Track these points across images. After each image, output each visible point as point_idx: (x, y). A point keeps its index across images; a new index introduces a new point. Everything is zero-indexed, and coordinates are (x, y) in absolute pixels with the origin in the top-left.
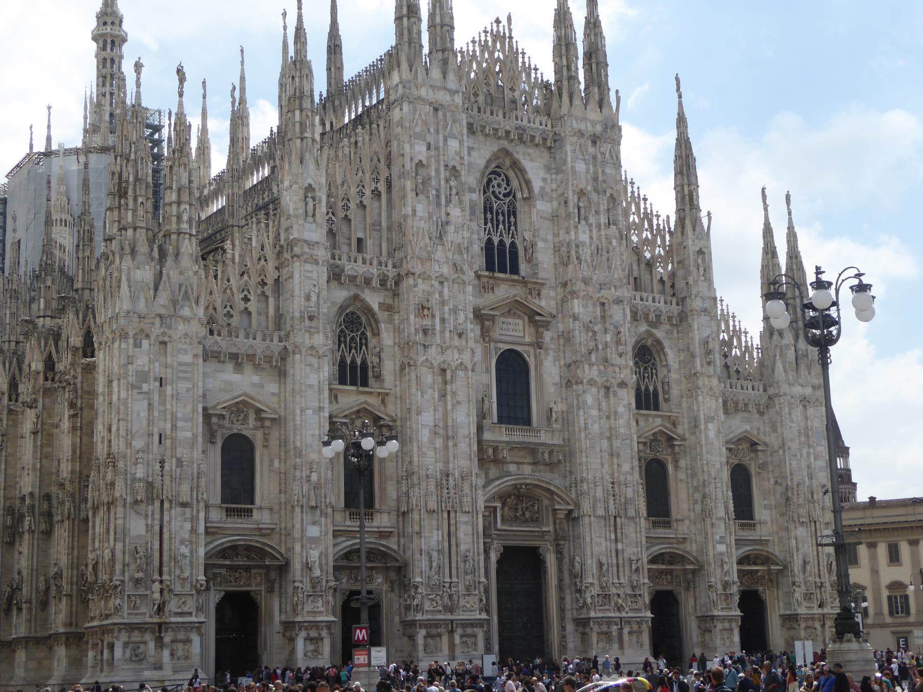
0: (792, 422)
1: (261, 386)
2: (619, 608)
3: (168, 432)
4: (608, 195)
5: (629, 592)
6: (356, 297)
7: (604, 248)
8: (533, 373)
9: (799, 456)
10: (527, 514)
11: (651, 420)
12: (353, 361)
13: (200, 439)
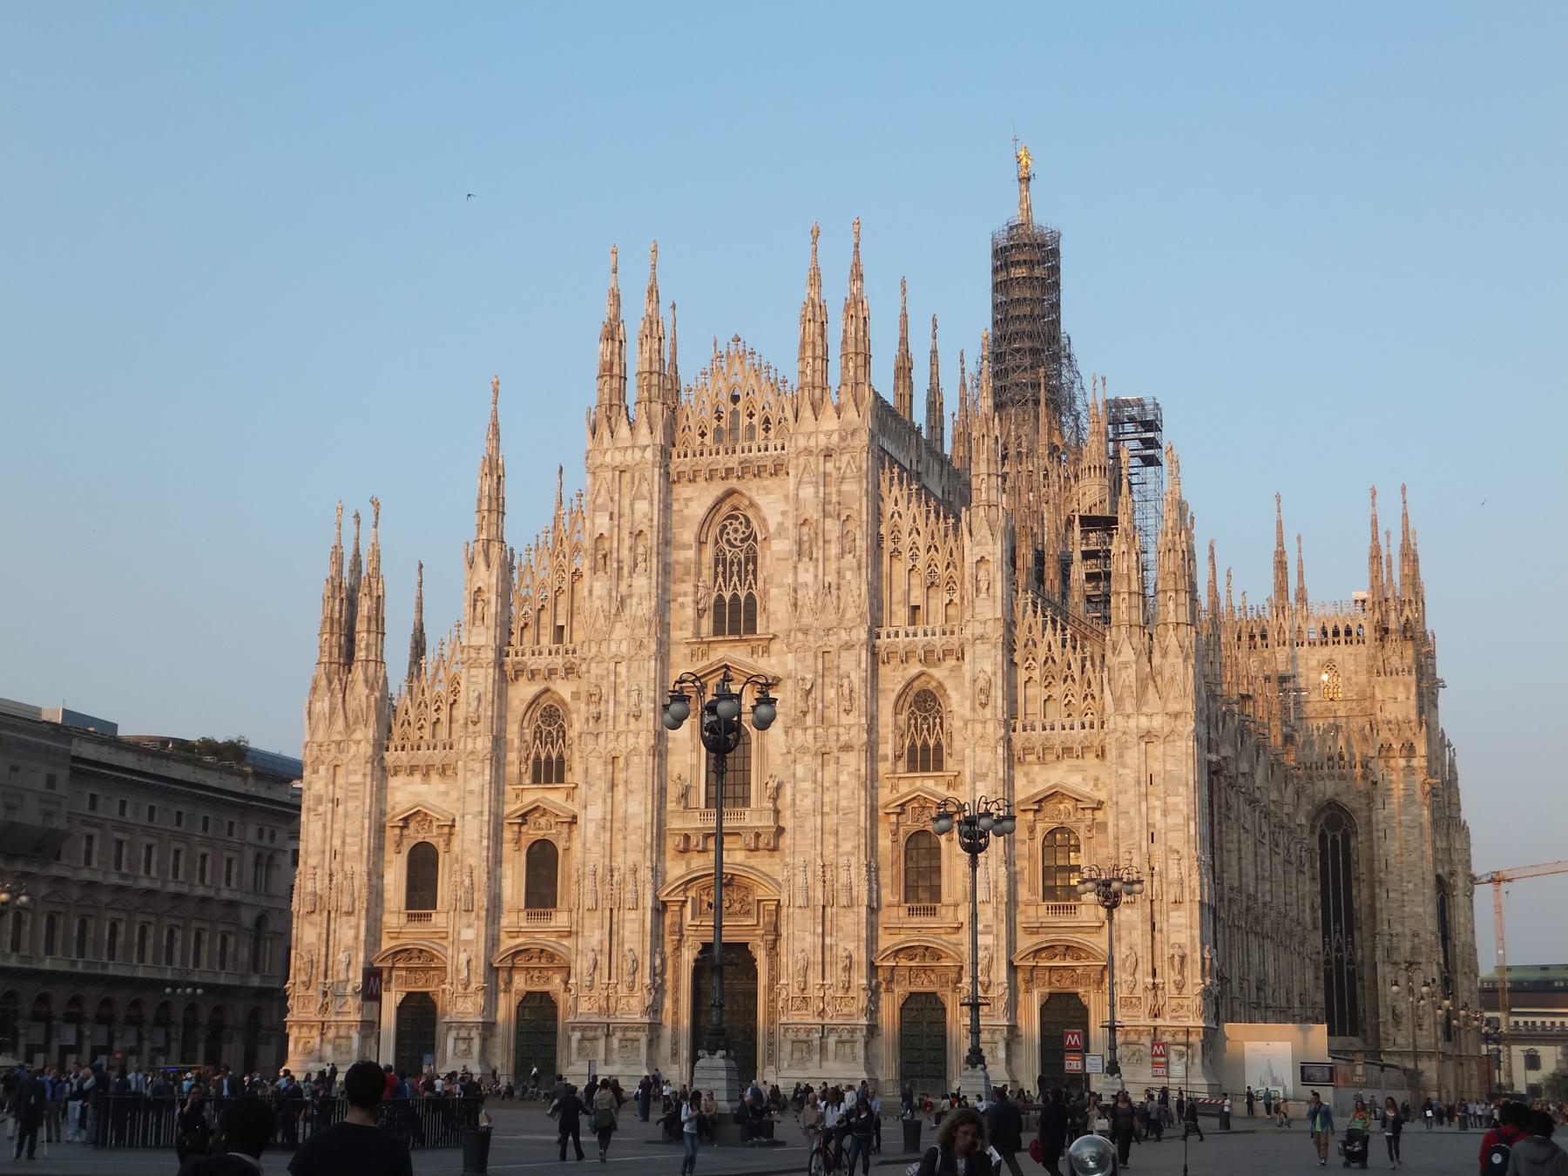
0: (1125, 766)
1: (447, 793)
2: (822, 1013)
3: (339, 849)
4: (843, 517)
5: (840, 994)
6: (547, 690)
7: (834, 586)
8: (754, 745)
9: (1132, 814)
10: (737, 906)
11: (918, 783)
12: (549, 757)
13: (365, 853)
